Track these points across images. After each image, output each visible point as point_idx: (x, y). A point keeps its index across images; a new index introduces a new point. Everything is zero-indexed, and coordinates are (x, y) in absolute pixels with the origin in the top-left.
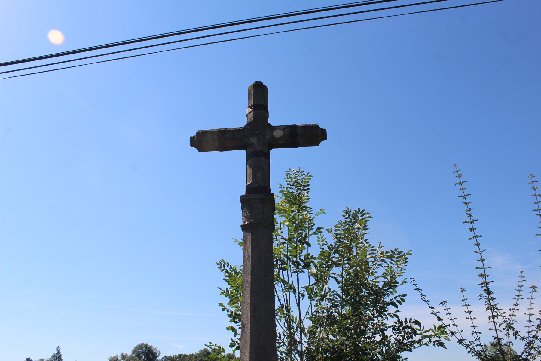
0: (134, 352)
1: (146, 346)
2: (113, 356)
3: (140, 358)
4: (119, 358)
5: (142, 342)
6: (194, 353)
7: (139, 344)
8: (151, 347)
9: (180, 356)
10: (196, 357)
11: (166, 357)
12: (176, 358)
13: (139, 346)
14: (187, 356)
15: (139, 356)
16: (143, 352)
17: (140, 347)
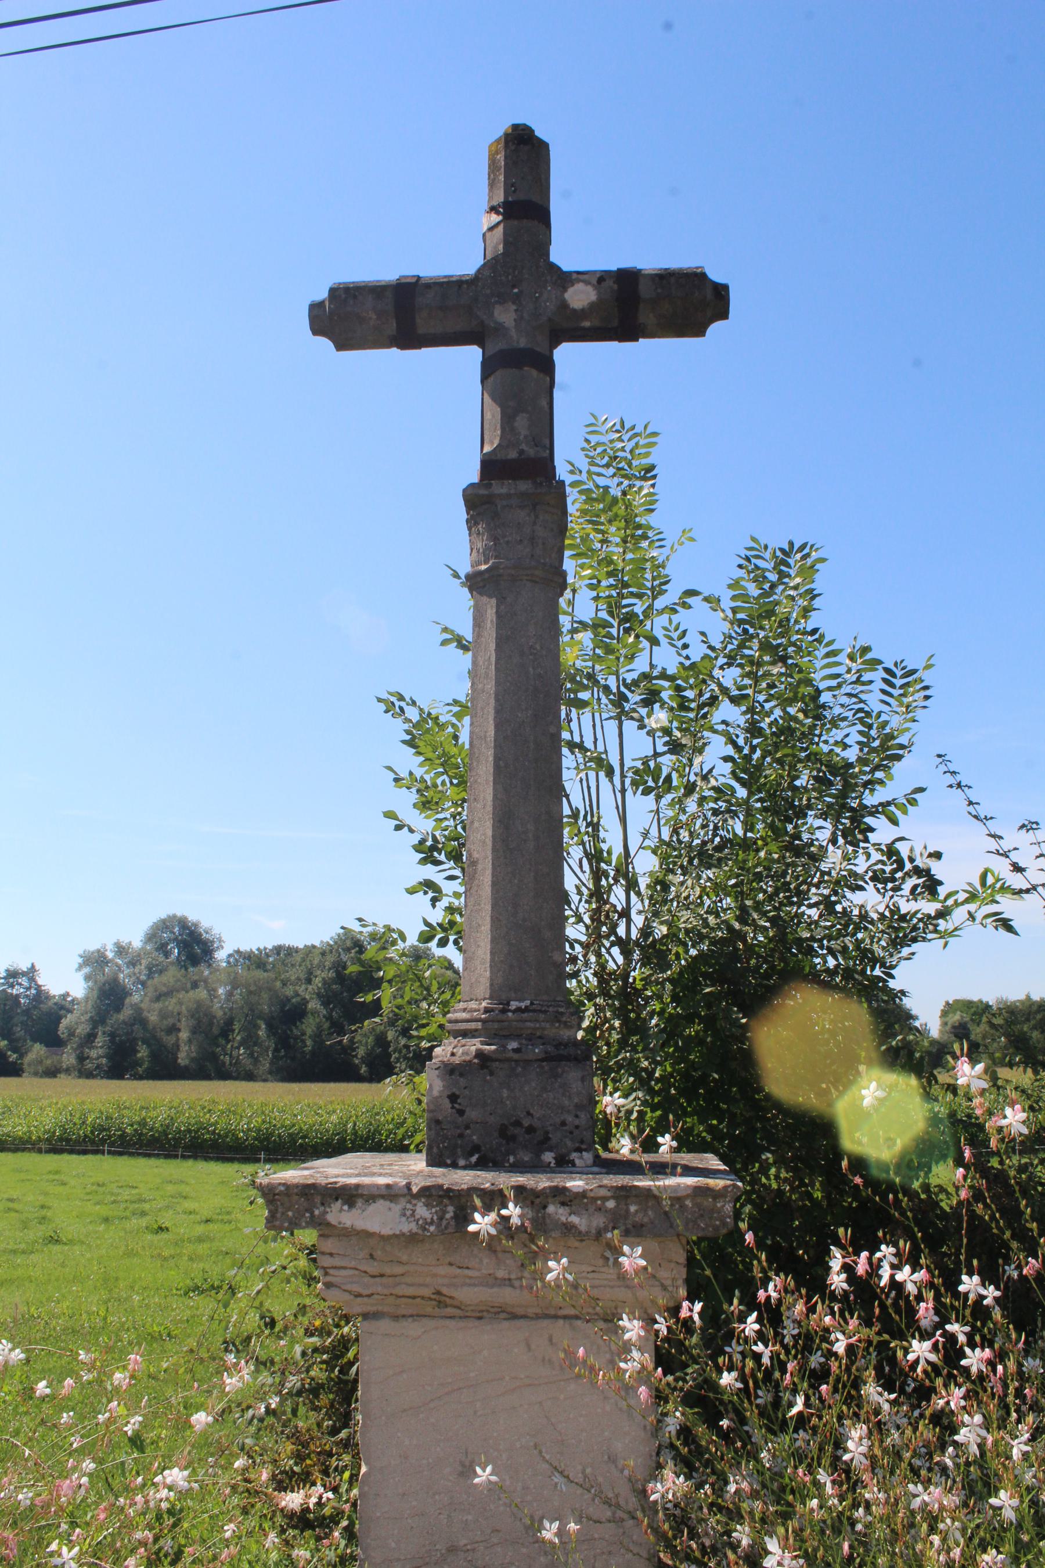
0: (152, 936)
1: (183, 923)
2: (93, 946)
3: (167, 954)
4: (110, 955)
5: (171, 913)
6: (317, 944)
7: (163, 916)
8: (196, 925)
9: (278, 949)
10: (323, 954)
11: (238, 952)
12: (268, 955)
13: (164, 921)
14: (297, 950)
15: (163, 948)
16: (176, 939)
17: (164, 925)
